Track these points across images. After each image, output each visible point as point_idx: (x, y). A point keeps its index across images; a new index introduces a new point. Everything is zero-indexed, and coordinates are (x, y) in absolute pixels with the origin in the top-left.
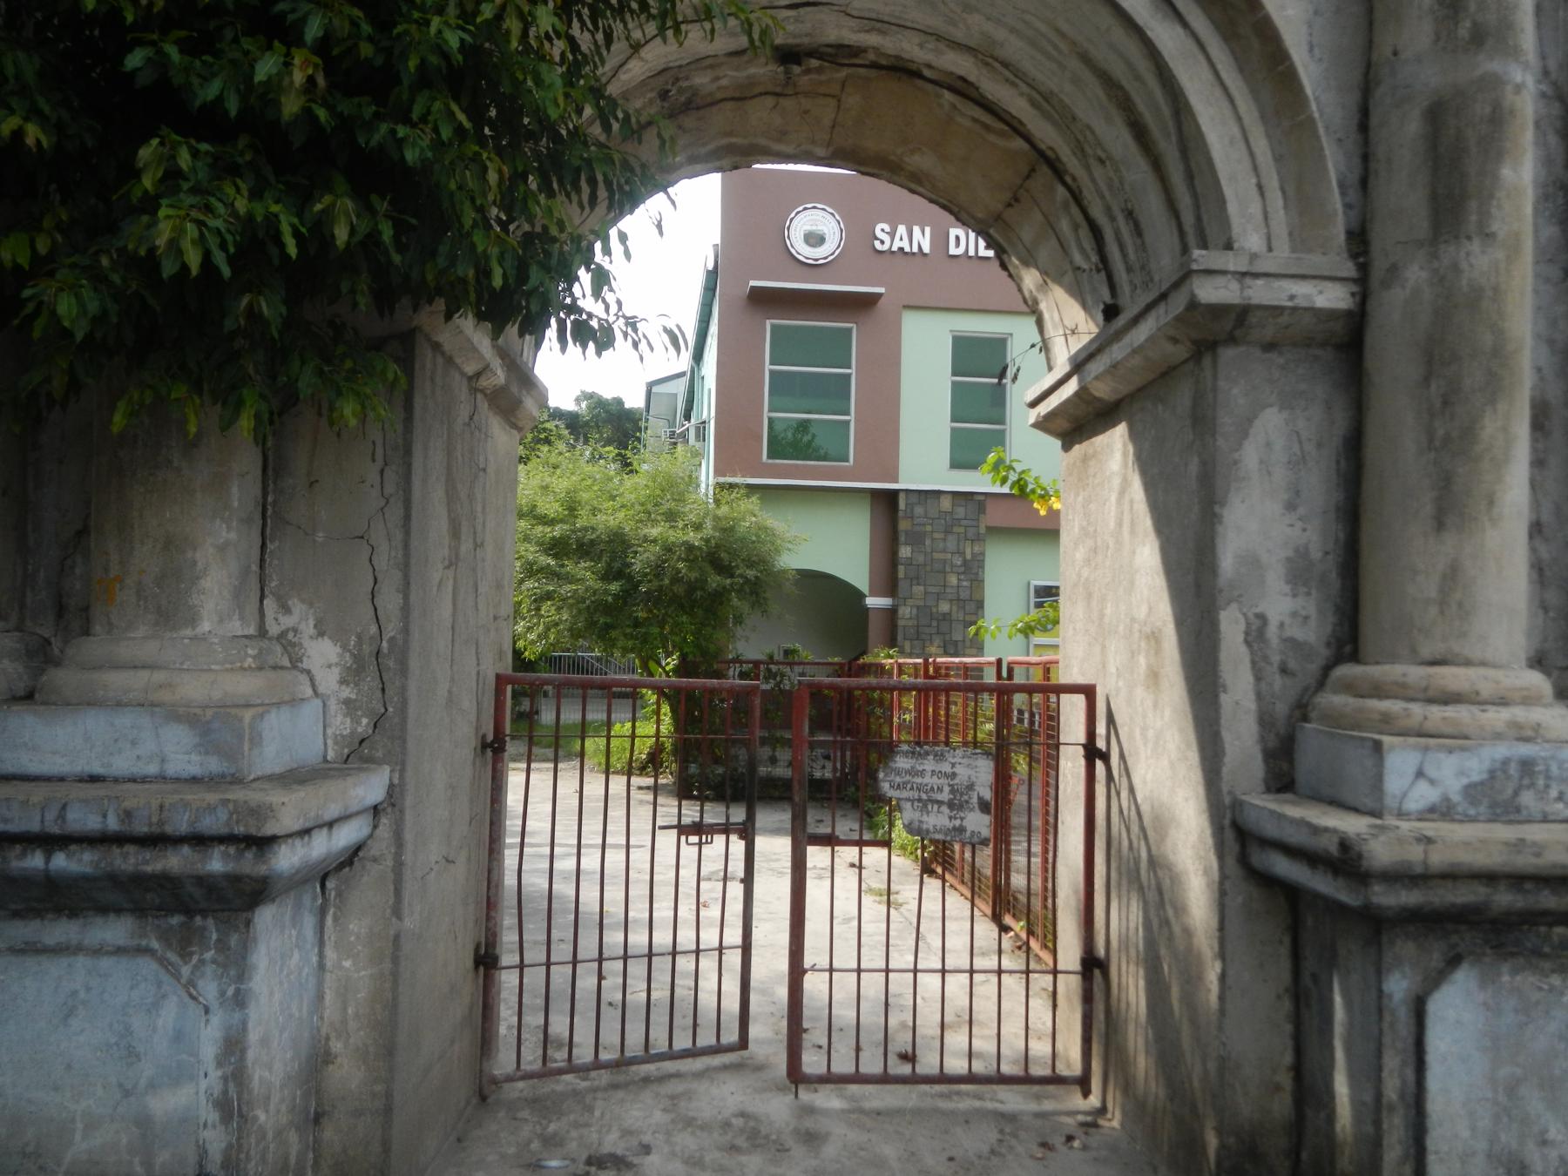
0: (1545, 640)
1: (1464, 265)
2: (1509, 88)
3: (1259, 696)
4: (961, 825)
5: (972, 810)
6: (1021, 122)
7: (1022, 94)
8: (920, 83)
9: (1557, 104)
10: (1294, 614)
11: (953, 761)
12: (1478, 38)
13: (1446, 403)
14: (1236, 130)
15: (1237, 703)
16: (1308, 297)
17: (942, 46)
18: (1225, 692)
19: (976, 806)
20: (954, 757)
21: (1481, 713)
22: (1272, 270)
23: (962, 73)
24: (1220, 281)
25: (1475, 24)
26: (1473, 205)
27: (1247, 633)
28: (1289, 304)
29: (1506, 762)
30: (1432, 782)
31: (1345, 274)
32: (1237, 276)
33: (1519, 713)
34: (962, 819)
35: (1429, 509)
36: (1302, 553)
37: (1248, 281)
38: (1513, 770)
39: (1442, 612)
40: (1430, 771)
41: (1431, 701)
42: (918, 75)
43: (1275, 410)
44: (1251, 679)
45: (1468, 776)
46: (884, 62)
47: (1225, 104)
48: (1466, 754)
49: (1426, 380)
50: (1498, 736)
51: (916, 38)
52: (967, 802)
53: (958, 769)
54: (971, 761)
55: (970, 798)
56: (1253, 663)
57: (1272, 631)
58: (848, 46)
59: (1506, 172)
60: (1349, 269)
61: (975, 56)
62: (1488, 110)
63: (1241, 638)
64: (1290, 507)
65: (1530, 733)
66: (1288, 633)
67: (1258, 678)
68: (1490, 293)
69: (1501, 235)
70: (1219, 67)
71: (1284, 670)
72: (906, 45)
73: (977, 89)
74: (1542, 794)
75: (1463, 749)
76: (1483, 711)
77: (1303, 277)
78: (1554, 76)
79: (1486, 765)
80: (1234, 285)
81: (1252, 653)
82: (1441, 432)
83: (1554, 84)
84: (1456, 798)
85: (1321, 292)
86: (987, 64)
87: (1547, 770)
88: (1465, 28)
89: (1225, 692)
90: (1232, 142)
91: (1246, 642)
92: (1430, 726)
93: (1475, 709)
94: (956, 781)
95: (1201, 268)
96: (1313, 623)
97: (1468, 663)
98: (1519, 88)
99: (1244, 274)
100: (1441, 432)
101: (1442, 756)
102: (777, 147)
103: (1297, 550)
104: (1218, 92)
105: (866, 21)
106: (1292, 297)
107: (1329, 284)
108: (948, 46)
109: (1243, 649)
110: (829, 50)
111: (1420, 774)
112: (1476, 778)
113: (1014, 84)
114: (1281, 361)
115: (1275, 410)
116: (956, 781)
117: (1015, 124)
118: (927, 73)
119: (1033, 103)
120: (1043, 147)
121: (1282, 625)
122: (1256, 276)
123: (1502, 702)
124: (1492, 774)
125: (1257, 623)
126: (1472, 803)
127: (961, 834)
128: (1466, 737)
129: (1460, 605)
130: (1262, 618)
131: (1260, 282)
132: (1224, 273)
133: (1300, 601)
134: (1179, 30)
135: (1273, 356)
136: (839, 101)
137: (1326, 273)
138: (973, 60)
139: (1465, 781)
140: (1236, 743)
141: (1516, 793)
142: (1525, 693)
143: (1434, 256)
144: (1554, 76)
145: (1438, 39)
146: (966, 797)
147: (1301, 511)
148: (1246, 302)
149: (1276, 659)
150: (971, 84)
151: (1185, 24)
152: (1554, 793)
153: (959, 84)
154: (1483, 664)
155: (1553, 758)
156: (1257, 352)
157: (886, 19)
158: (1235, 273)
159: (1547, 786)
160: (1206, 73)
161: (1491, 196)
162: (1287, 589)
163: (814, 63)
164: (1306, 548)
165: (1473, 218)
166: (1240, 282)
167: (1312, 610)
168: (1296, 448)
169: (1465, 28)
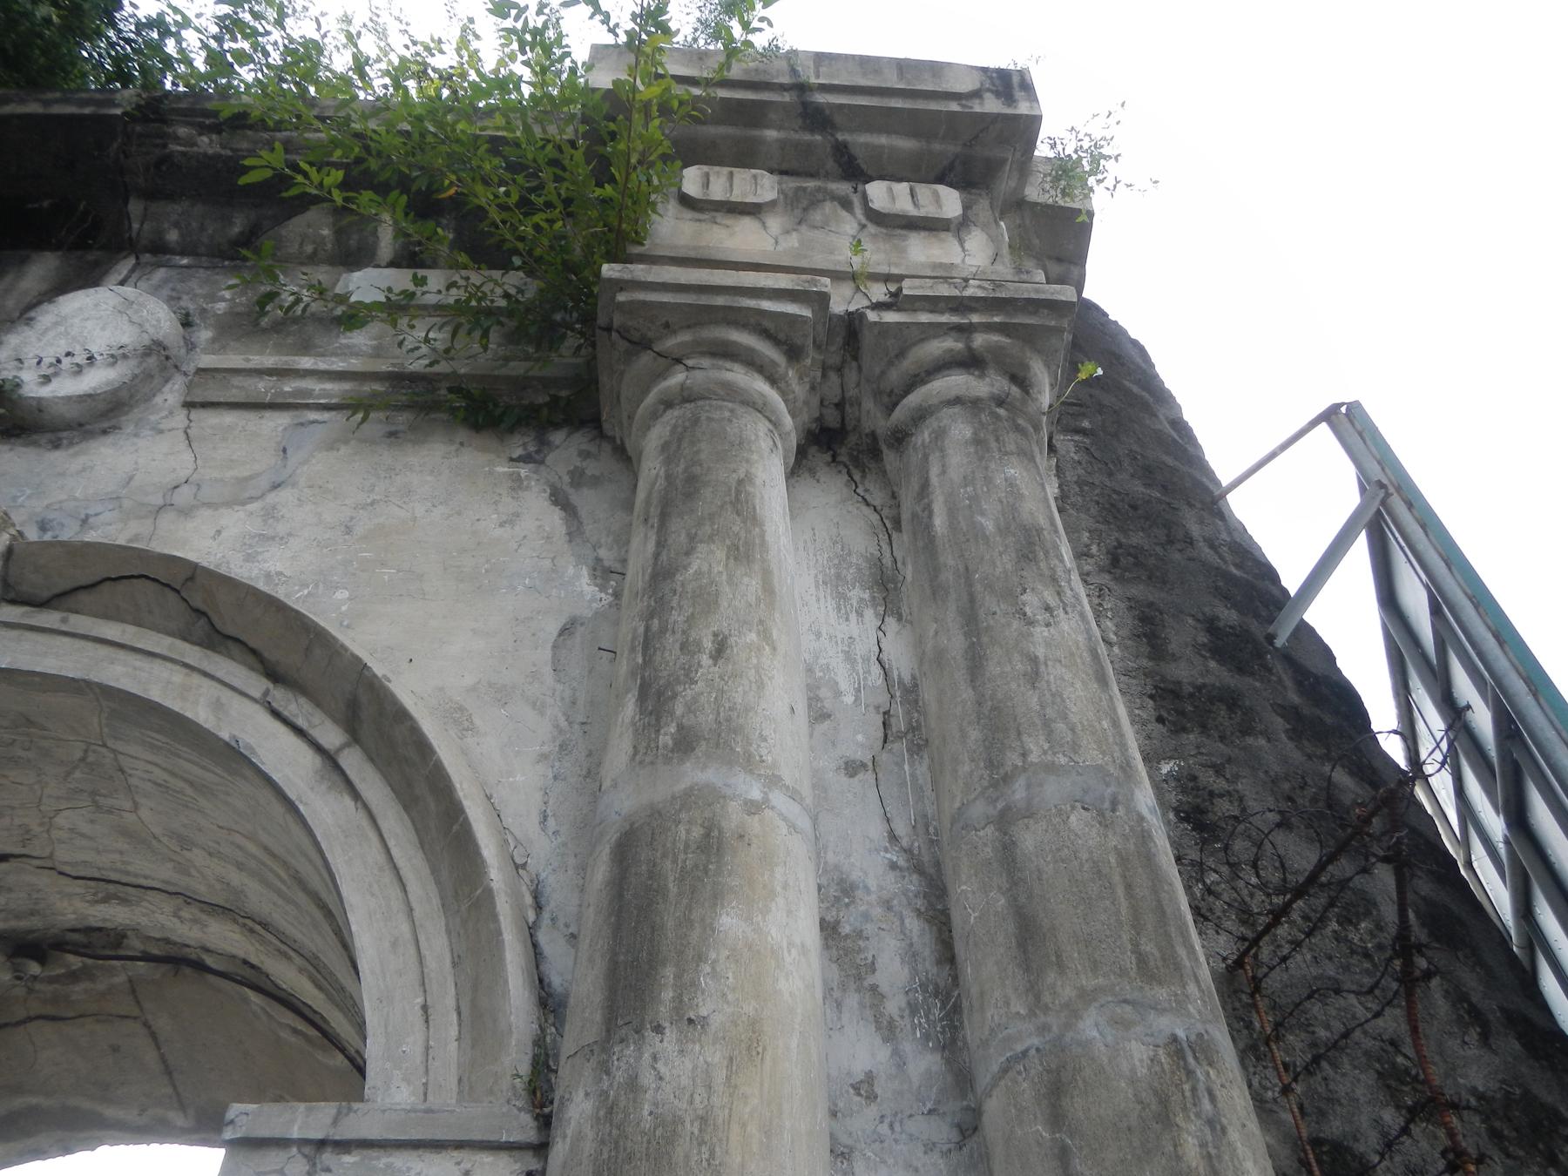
1: (647, 1079)
2: (734, 807)
8: (211, 978)
9: (915, 877)
12: (686, 743)
14: (405, 928)
23: (241, 954)
25: (680, 727)
26: (669, 972)
31: (515, 1137)
32: (307, 1150)
37: (328, 1157)
42: (200, 967)
46: (155, 951)
47: (394, 892)
51: (168, 905)
58: (100, 929)
59: (729, 922)
60: (523, 1128)
61: (235, 921)
62: (697, 832)
69: (716, 1021)
70: (391, 843)
72: (162, 918)
77: (437, 1146)
78: (905, 842)
83: (908, 851)
86: (252, 931)
88: (666, 738)
90: (394, 944)
98: (753, 808)
99: (322, 1144)
102: (110, 1112)
104: (388, 877)
105: (92, 883)
107: (486, 1158)
110: (76, 937)
113: (289, 958)
117: (320, 1022)
118: (209, 961)
122: (344, 1146)
134: (348, 802)
136: (146, 1025)
137: (477, 1136)
143: (605, 1069)
144: (905, 842)
145: (636, 752)
151: (356, 795)
157: (114, 876)
160: (375, 854)
161: (700, 958)
163: (75, 961)
165: (667, 995)
166: (312, 1161)
169: (666, 738)
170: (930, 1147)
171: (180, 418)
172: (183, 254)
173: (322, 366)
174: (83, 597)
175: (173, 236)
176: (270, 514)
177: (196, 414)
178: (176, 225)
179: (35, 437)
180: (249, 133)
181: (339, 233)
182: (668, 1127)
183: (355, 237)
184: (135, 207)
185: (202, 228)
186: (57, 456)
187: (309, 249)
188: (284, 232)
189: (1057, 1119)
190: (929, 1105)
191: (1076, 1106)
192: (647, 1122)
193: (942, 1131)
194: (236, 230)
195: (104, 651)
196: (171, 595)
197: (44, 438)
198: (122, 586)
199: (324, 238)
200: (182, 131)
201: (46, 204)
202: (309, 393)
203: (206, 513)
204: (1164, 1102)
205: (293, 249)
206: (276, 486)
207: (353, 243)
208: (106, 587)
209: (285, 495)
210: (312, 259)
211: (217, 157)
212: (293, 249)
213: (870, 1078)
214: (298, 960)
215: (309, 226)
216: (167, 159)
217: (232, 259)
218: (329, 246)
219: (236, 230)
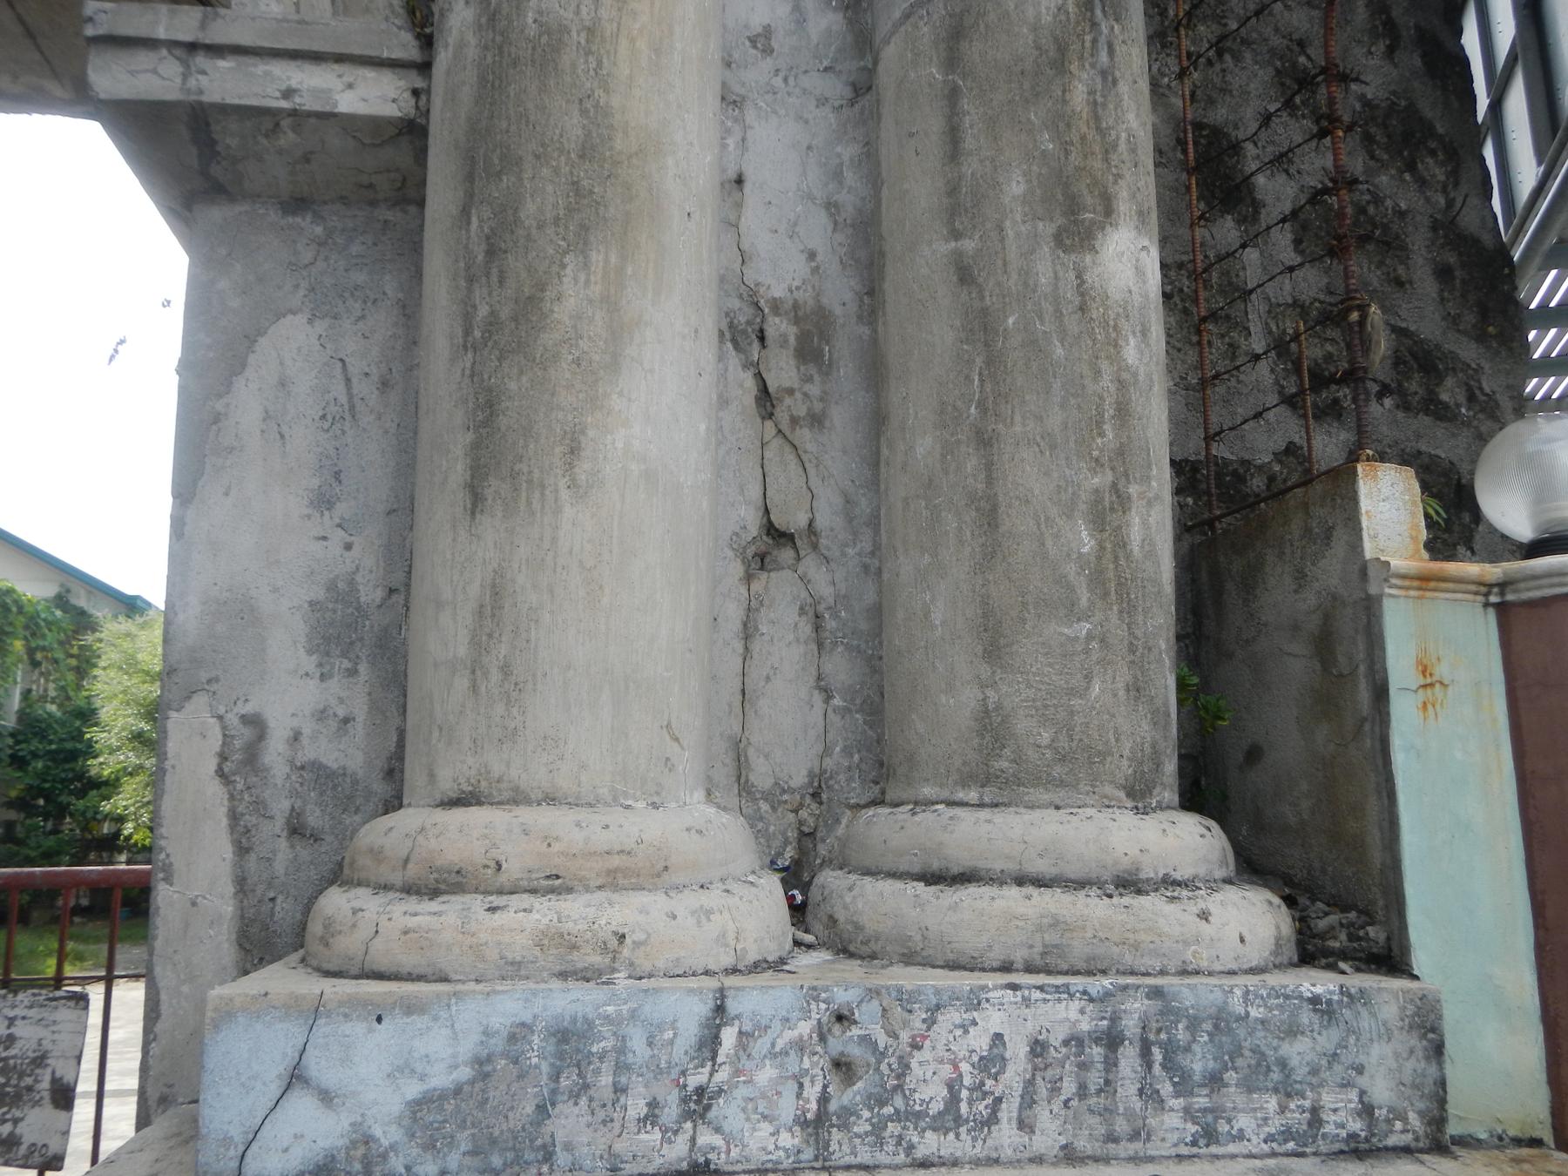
0: (827, 751)
3: (241, 883)
4: (11, 1134)
5: (37, 1103)
10: (321, 715)
11: (11, 1014)
13: (491, 253)
15: (194, 904)
16: (316, 93)
18: (168, 880)
19: (46, 1095)
20: (14, 1007)
21: (488, 915)
22: (246, 40)
24: (143, 59)
27: (223, 757)
28: (284, 104)
29: (519, 1034)
30: (326, 1097)
31: (397, 54)
32: (178, 52)
33: (576, 912)
34: (16, 1121)
35: (459, 471)
36: (342, 593)
37: (201, 60)
38: (537, 1052)
39: (474, 688)
40: (320, 1067)
41: (410, 890)
43: (301, 319)
44: (227, 851)
45: (423, 1077)
48: (419, 1021)
49: (465, 212)
50: (514, 970)
52: (30, 1089)
53: (20, 1030)
54: (45, 1013)
55: (36, 1081)
56: (234, 816)
57: (275, 753)
60: (404, 45)
63: (212, 764)
64: (323, 502)
65: (597, 959)
66: (308, 753)
67: (242, 850)
68: (577, 37)
71: (296, 829)
74: (607, 1113)
75: (411, 1008)
76: (493, 910)
77: (317, 57)
79: (468, 1046)
80: (171, 68)
81: (232, 797)
82: (483, 311)
84: (387, 1134)
85: (350, 86)
87: (621, 1050)
89: (168, 880)
91: (220, 773)
92: (385, 953)
93: (477, 903)
94: (12, 1052)
95: (101, 32)
96: (359, 728)
97: (518, 798)
99: (193, 47)
100: (483, 311)
101: (357, 1029)
103: (331, 587)
106: (288, 93)
107: (369, 73)
109: (215, 791)
111: (296, 1078)
112: (441, 1079)
114: (319, 230)
115: (301, 319)
116: (12, 1052)
121: (296, 737)
122: (217, 50)
123: (554, 885)
124: (483, 1065)
125: (245, 734)
126: (430, 1146)
127: (9, 1151)
128: (445, 979)
129: (506, 670)
130: (255, 722)
131: (224, 64)
132: (150, 43)
133: (335, 685)
135: (304, 221)
137: (356, 51)
139: (413, 1090)
140: (185, 989)
141: (542, 1110)
142: (616, 861)
146: (29, 1081)
147: (342, 509)
148: (193, 98)
149: (281, 807)
152: (636, 1106)
154: (550, 799)
155: (633, 1014)
156: (274, 216)
158: (173, 44)
159: (620, 1090)
162: (309, 663)
164: (352, 583)
166: (185, 64)
167: (360, 708)
168: (339, 390)
170: (822, 102)
182: (552, 38)
189: (952, 62)
190: (826, 63)
191: (973, 50)
192: (532, 29)
193: (836, 88)
204: (1062, 50)
213: (767, 32)
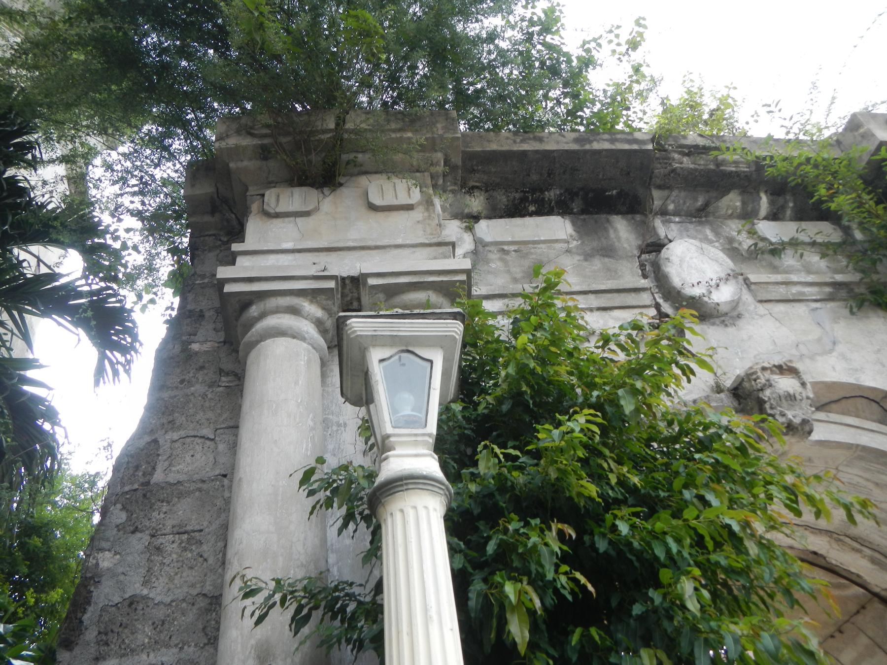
6: (858, 576)
7: (864, 557)
17: (807, 533)
23: (815, 549)
61: (831, 537)
73: (825, 558)
108: (812, 532)
117: (854, 578)
119: (873, 561)
120: (877, 590)
138: (828, 539)
150: (821, 556)
153: (811, 558)
171: (762, 309)
172: (674, 215)
173: (803, 280)
174: (834, 406)
175: (671, 207)
176: (843, 356)
177: (769, 306)
178: (673, 202)
179: (712, 321)
180: (704, 156)
181: (744, 203)
183: (751, 206)
184: (656, 193)
185: (685, 203)
186: (731, 330)
187: (730, 212)
188: (720, 204)
194: (700, 203)
195: (853, 430)
196: (874, 405)
197: (717, 321)
198: (850, 401)
199: (737, 207)
200: (676, 156)
201: (614, 192)
202: (803, 294)
203: (819, 358)
205: (723, 212)
206: (834, 343)
207: (749, 209)
208: (844, 401)
209: (840, 348)
210: (731, 217)
211: (696, 170)
212: (723, 212)
214: (868, 552)
215: (731, 201)
216: (674, 171)
217: (695, 217)
218: (739, 211)
219: (700, 203)
